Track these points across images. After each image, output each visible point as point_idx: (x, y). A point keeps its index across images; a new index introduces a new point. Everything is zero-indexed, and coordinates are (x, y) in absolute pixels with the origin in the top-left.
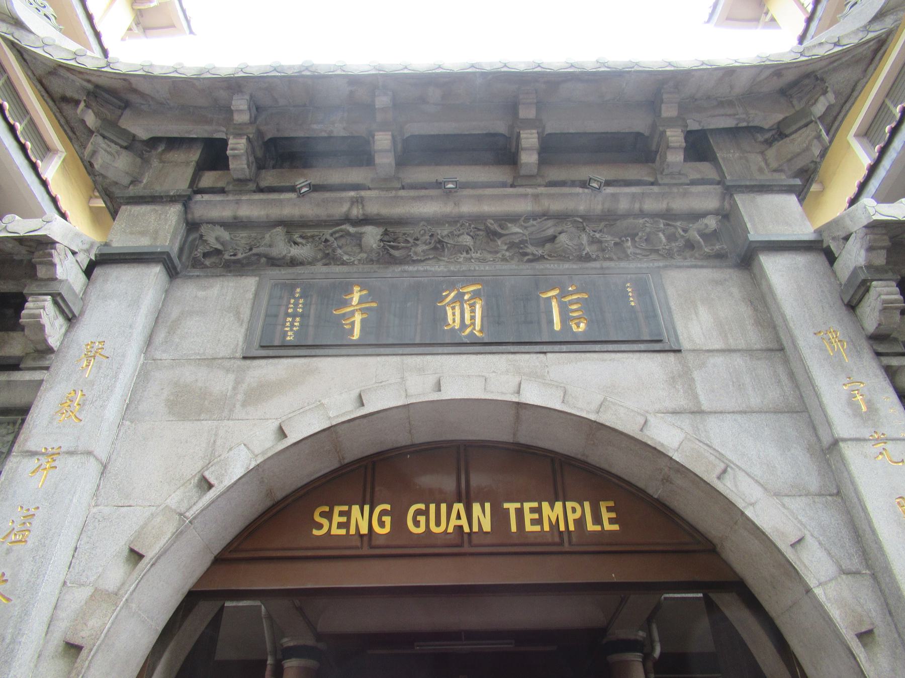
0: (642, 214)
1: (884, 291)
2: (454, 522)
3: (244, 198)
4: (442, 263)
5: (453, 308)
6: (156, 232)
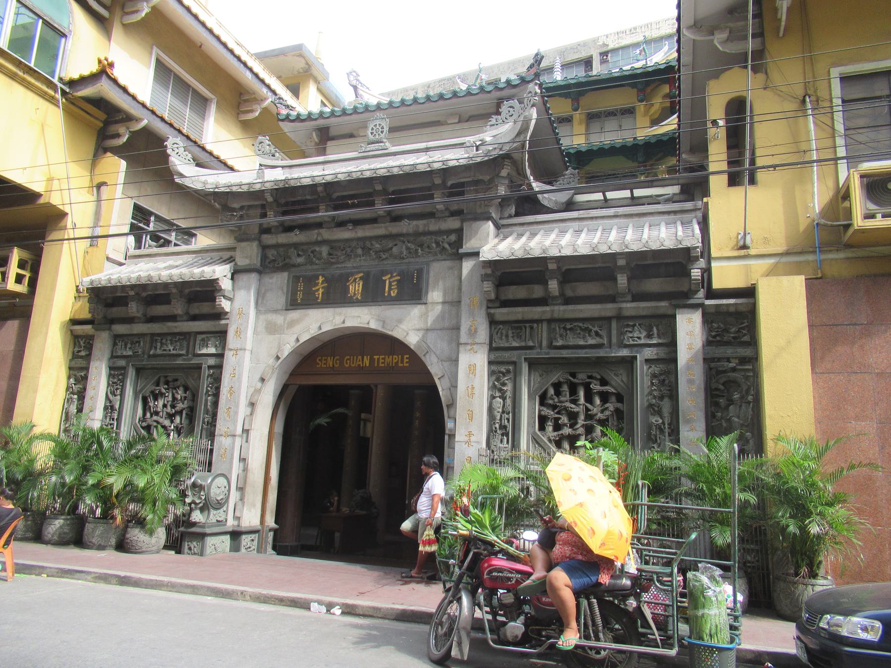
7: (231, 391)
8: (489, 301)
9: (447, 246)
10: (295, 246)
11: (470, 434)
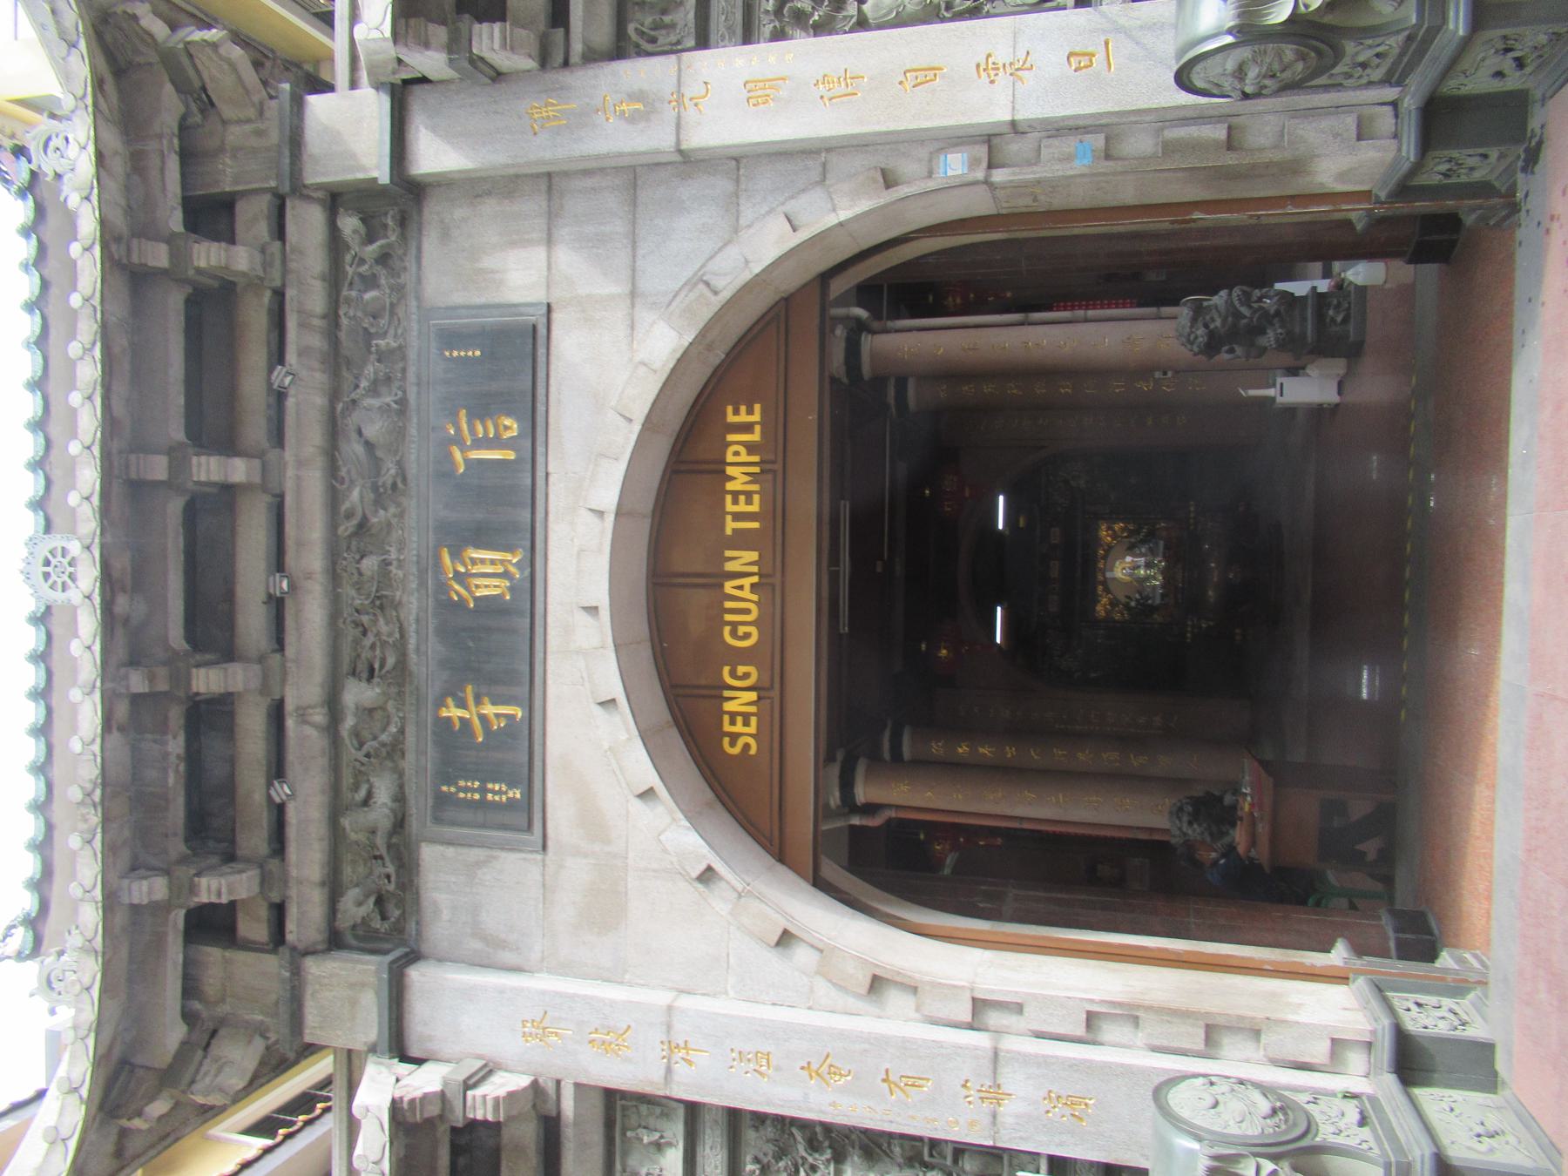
0: (332, 317)
1: (488, 40)
2: (746, 594)
3: (294, 872)
4: (405, 599)
5: (477, 586)
6: (352, 986)
7: (822, 1070)
8: (544, 61)
9: (372, 248)
10: (335, 813)
11: (987, 68)
